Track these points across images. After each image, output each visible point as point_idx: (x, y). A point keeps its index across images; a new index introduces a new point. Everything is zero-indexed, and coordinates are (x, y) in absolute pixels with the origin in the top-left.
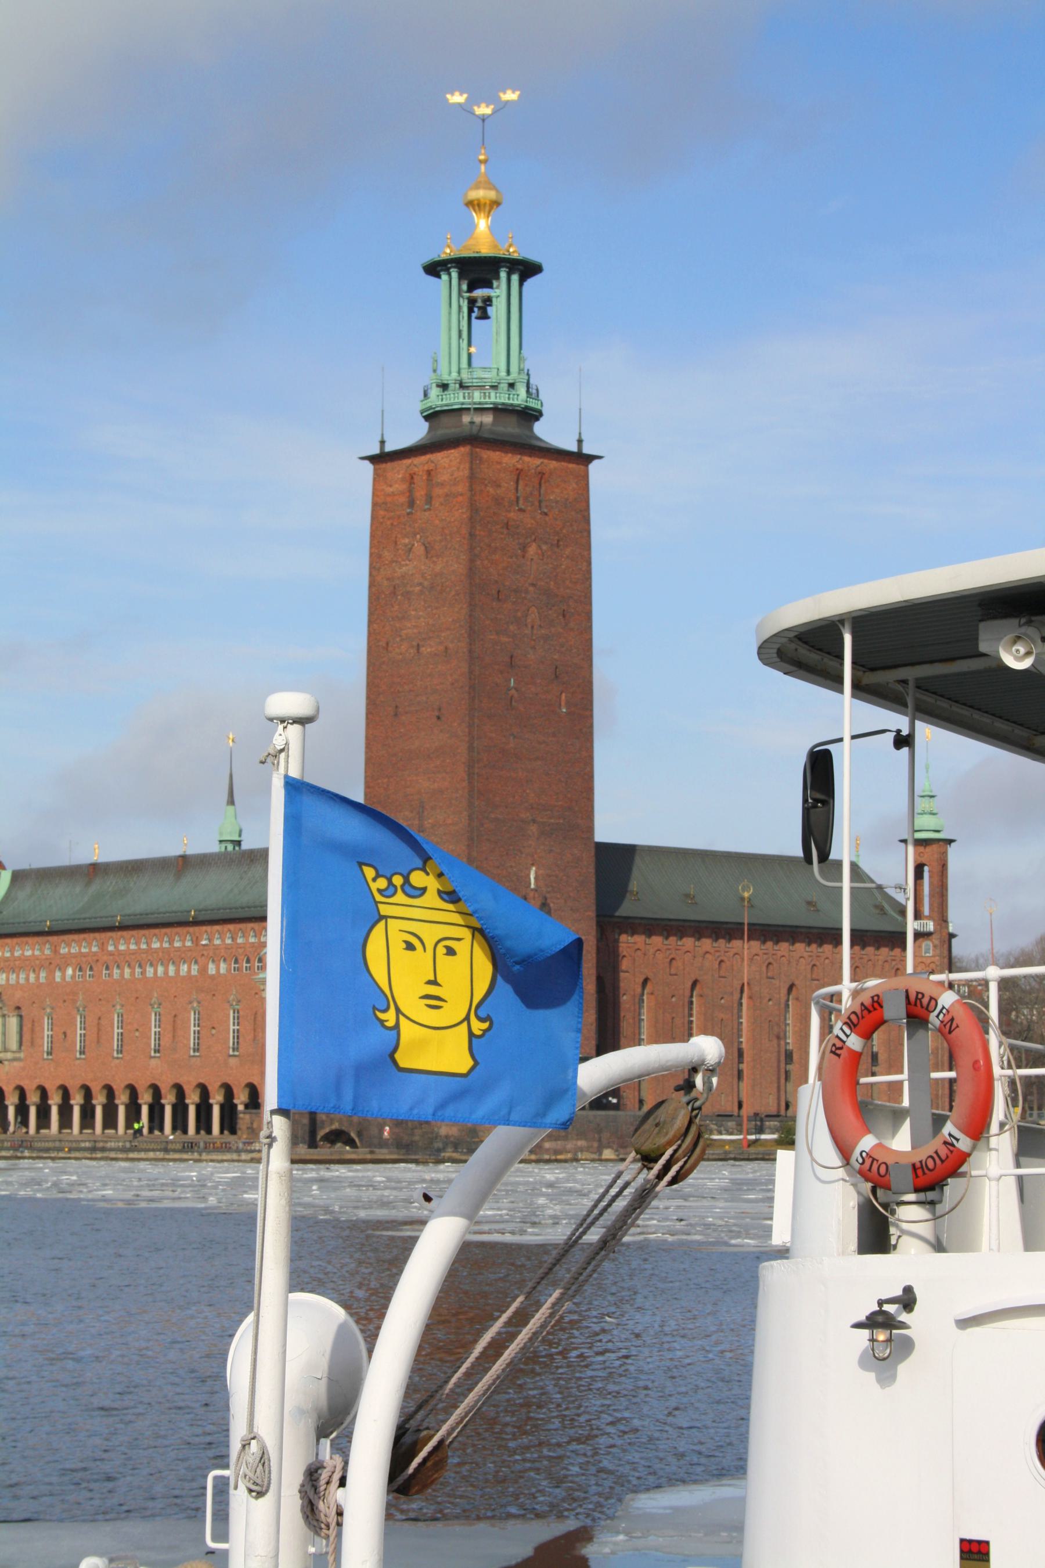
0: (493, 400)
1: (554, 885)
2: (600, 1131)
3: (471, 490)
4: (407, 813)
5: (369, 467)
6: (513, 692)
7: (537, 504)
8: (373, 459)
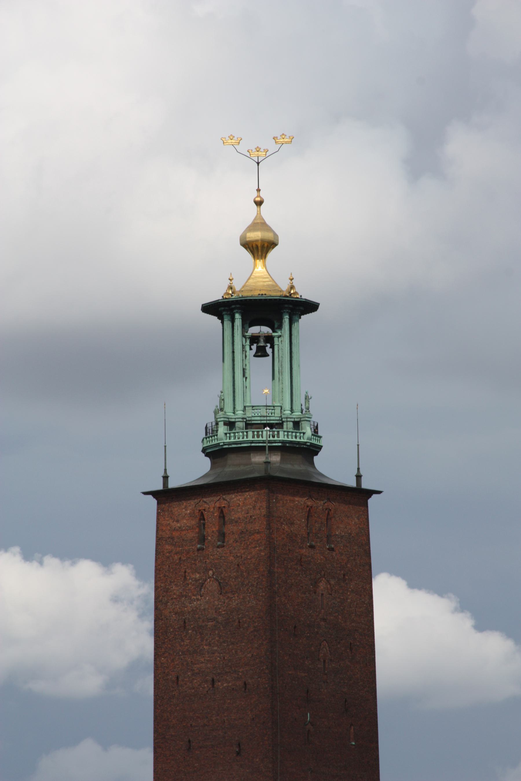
0: (281, 438)
5: (152, 502)
7: (325, 539)
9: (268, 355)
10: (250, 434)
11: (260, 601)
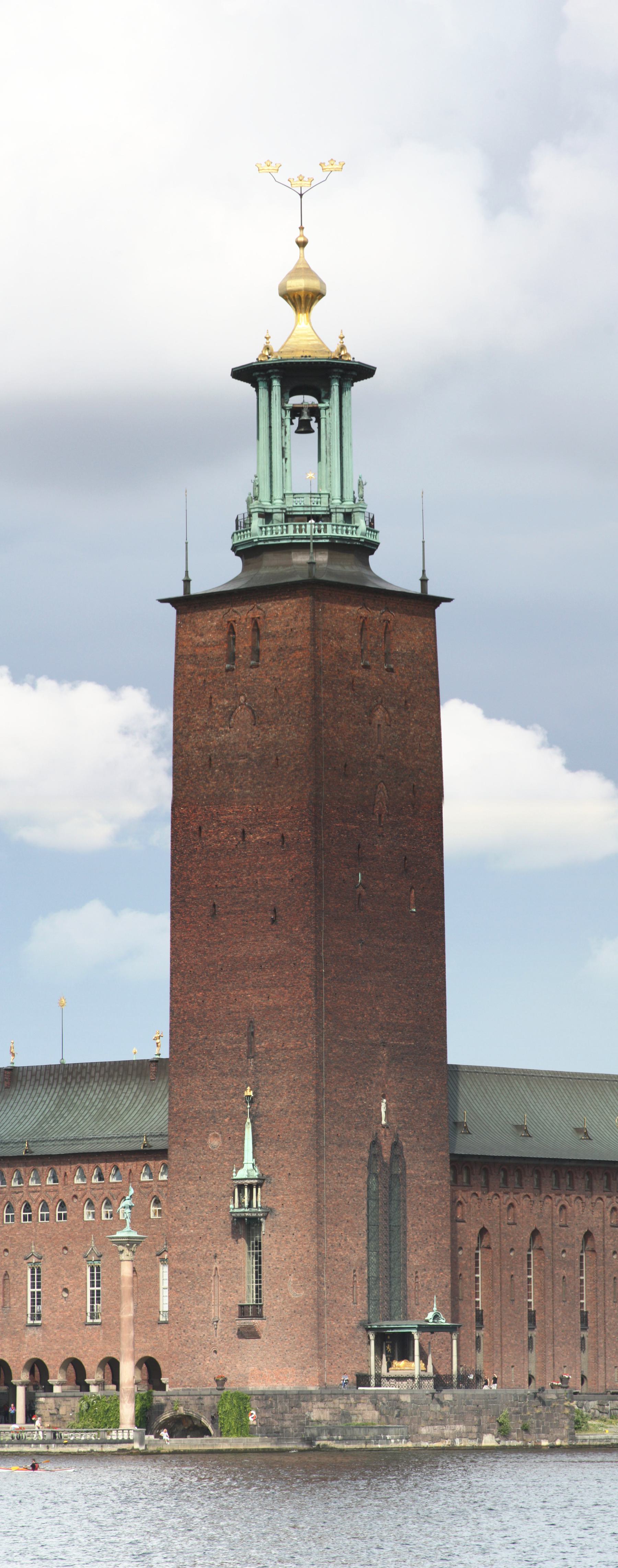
0: (329, 533)
1: (406, 1120)
2: (479, 1414)
3: (314, 645)
4: (231, 1035)
5: (171, 611)
6: (361, 889)
7: (382, 657)
8: (174, 602)
9: (313, 431)
10: (291, 528)
11: (302, 734)
